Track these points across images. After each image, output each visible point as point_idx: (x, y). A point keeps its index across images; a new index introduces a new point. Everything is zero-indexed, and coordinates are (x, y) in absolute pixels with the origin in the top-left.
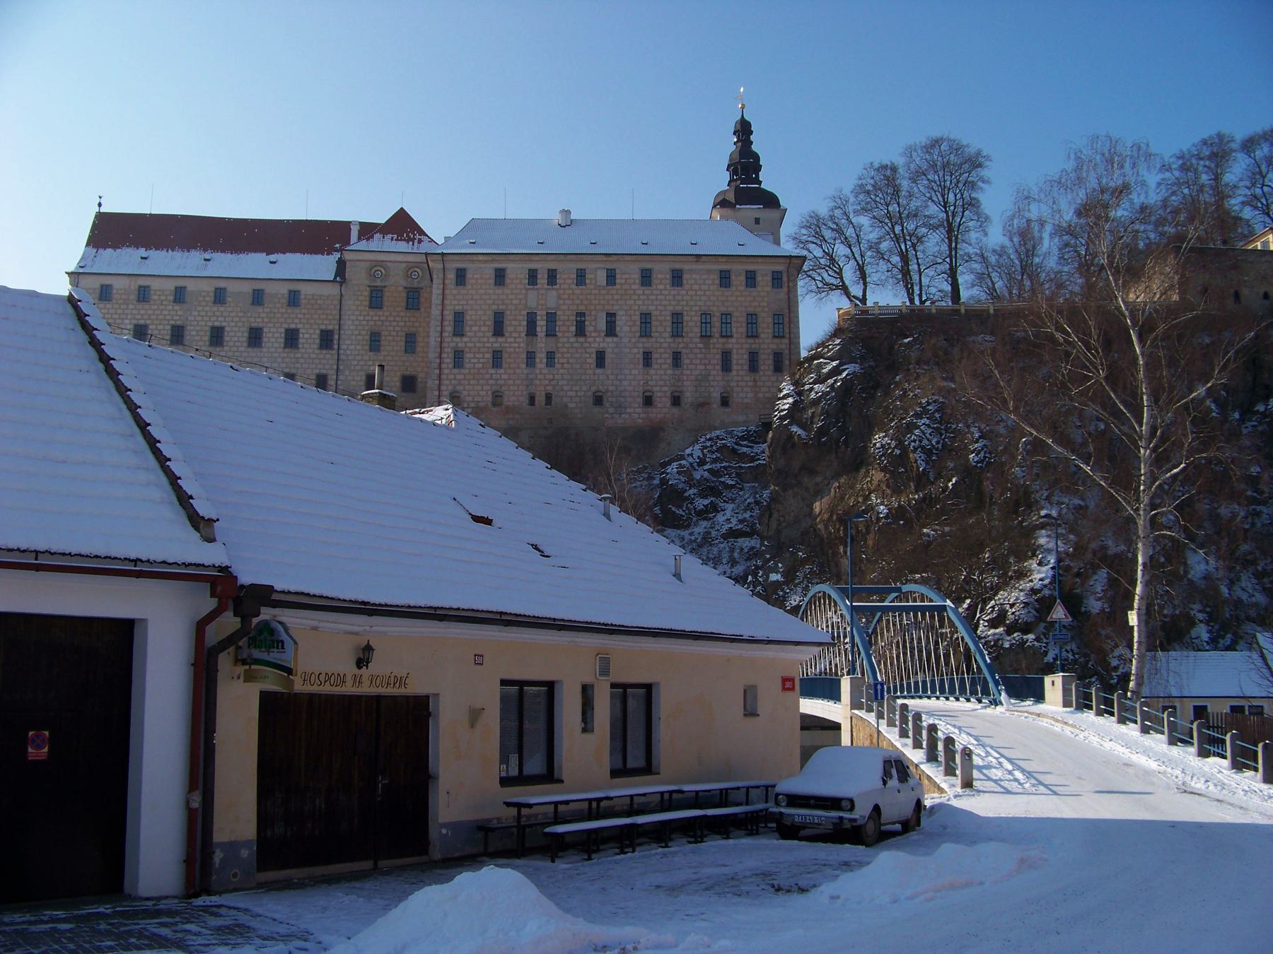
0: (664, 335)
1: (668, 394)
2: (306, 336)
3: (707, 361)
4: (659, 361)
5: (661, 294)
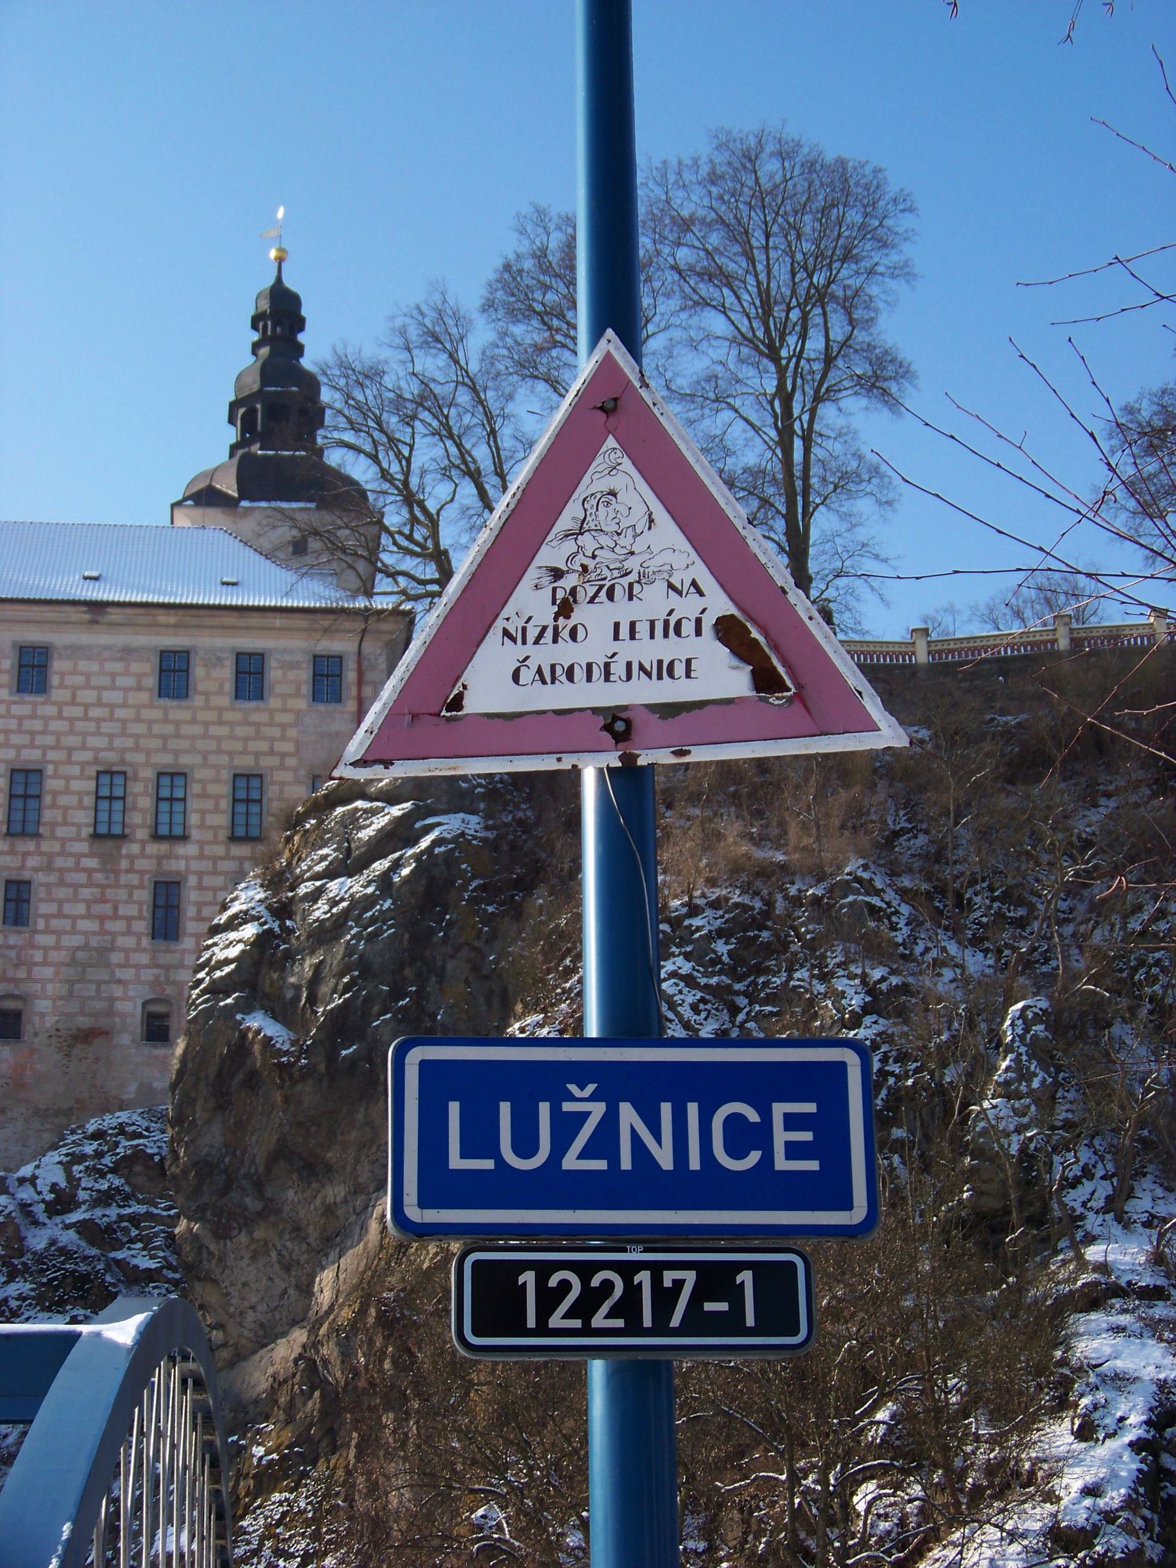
3: (107, 909)
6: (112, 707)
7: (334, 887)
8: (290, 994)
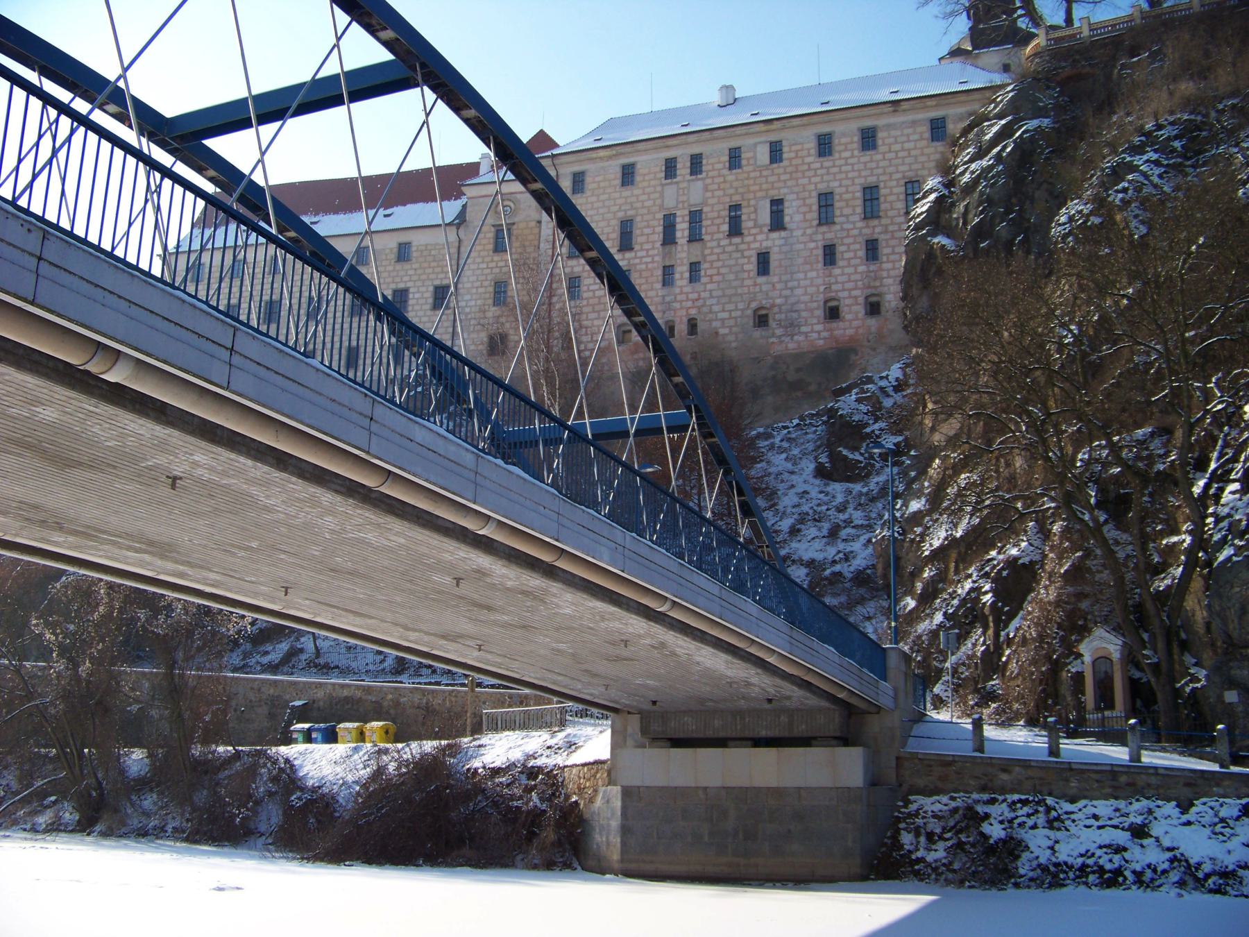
0: (852, 219)
1: (861, 300)
2: (417, 296)
4: (846, 255)
5: (847, 164)
6: (909, 150)
7: (973, 166)
8: (954, 223)
